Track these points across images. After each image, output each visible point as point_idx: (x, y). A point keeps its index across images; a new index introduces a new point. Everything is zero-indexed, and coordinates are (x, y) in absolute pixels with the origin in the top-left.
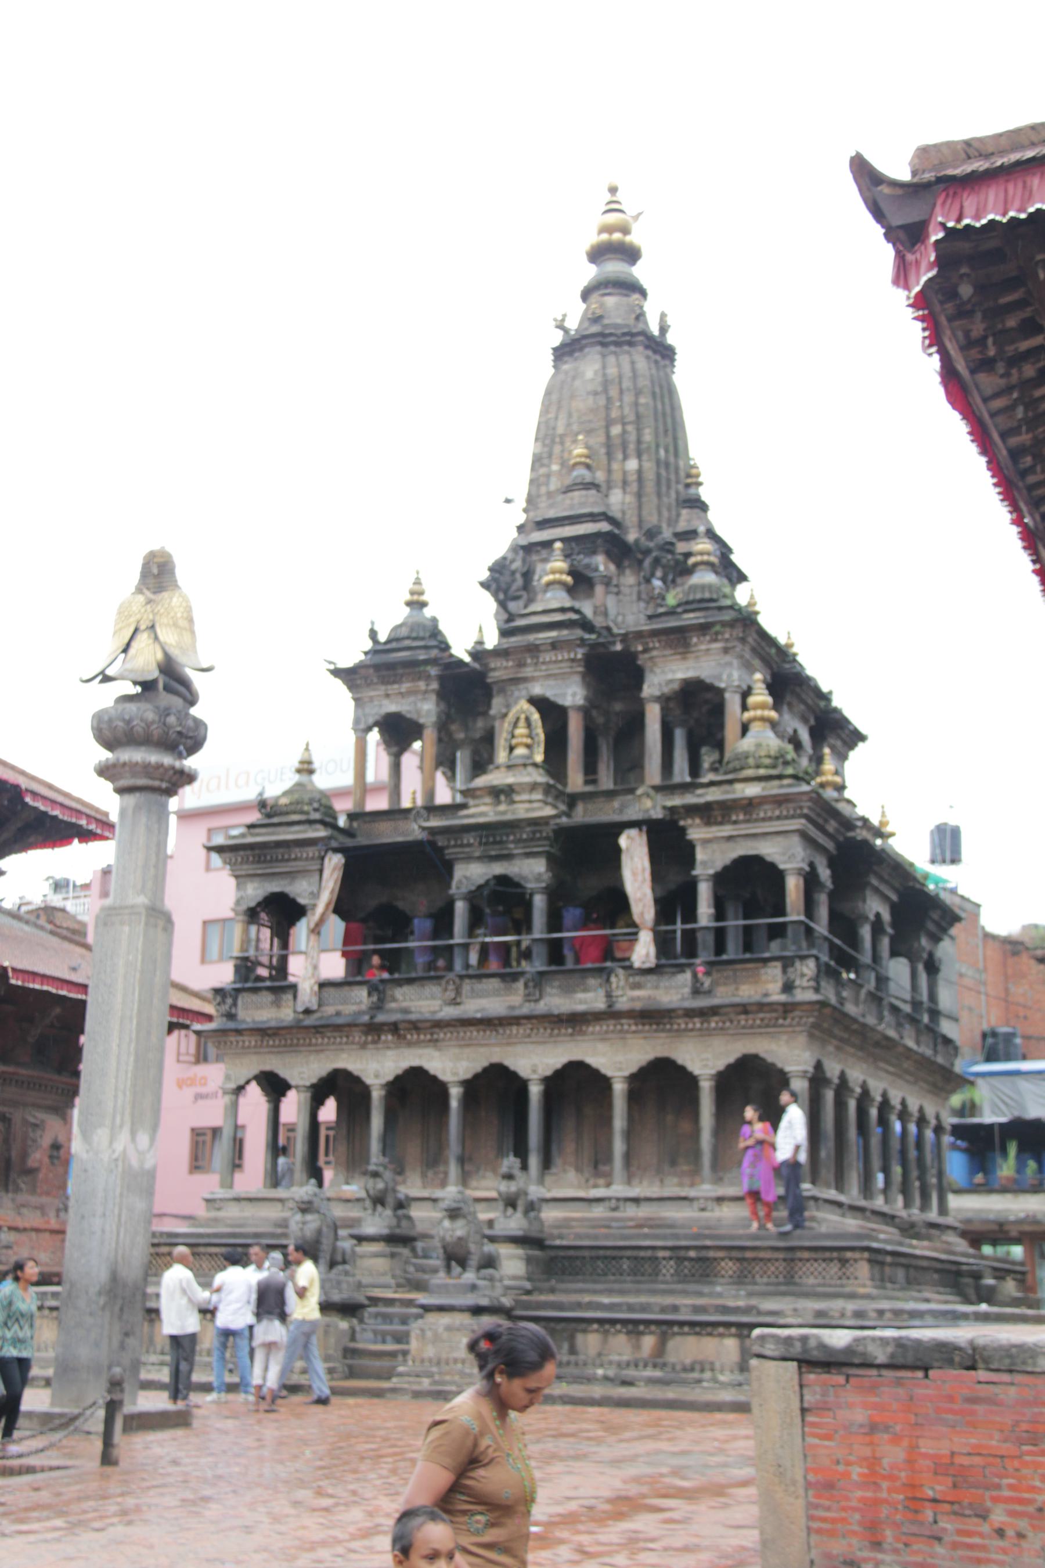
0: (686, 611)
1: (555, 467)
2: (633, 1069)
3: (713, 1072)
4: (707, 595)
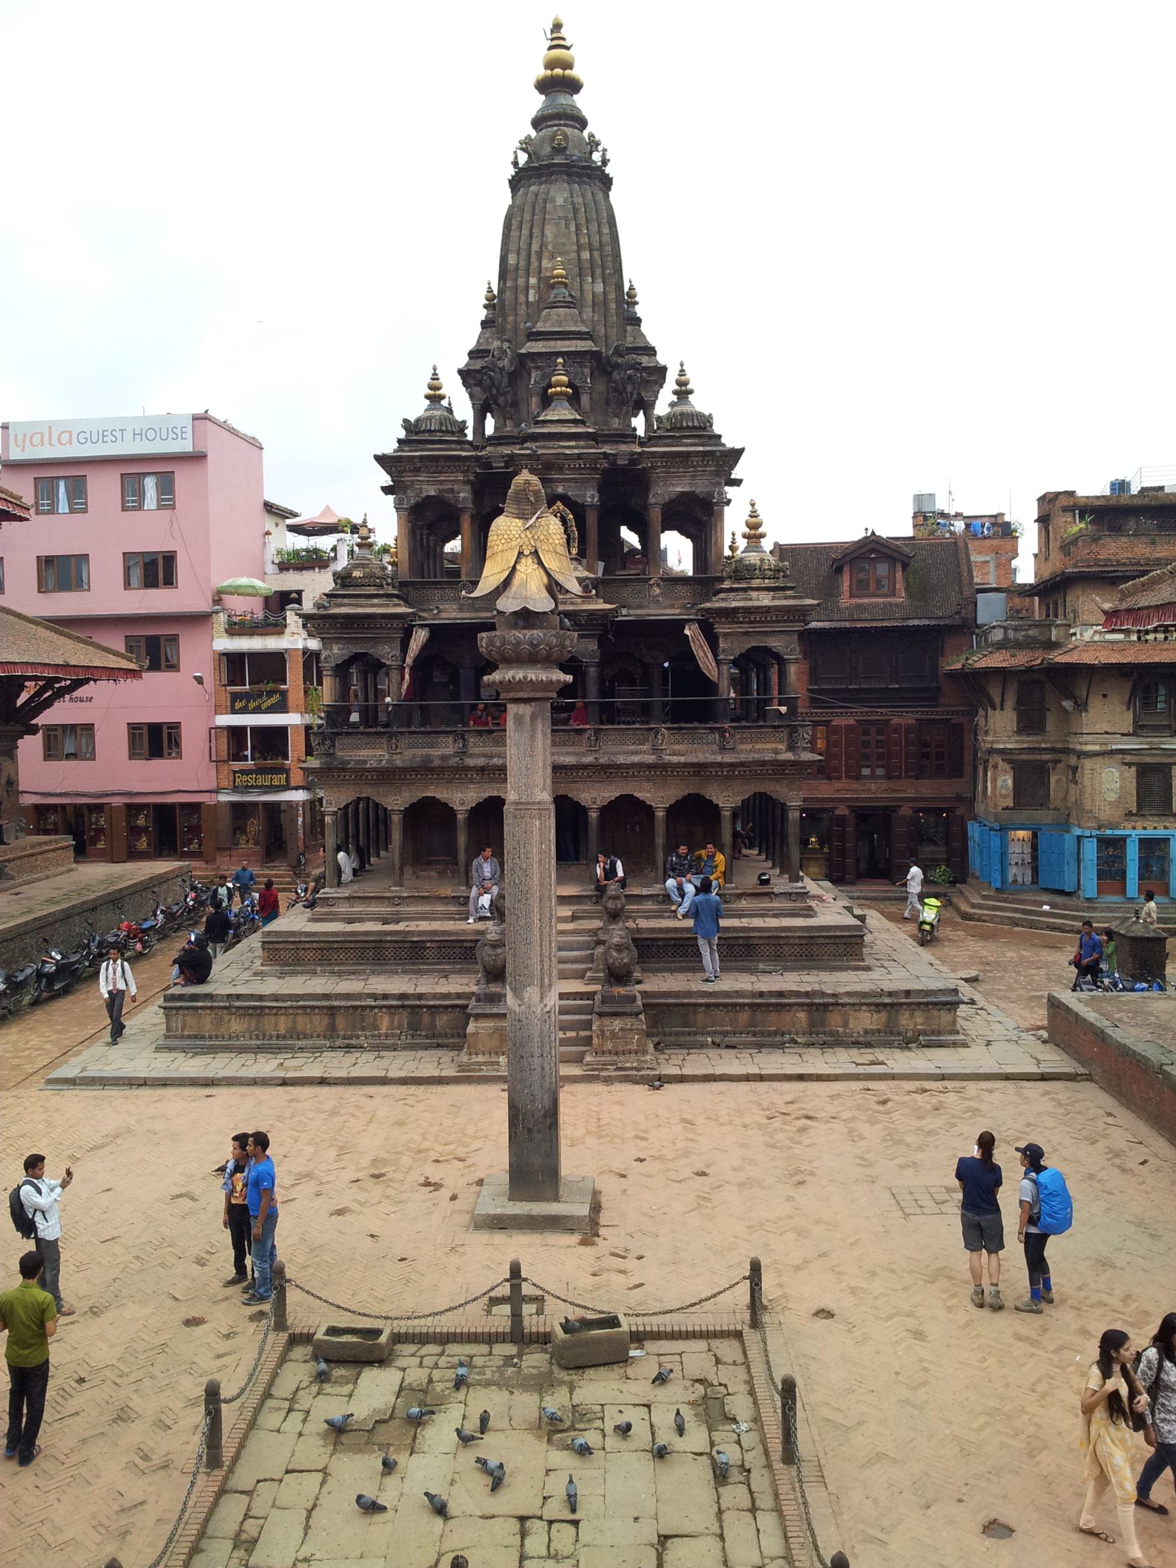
1: (533, 281)
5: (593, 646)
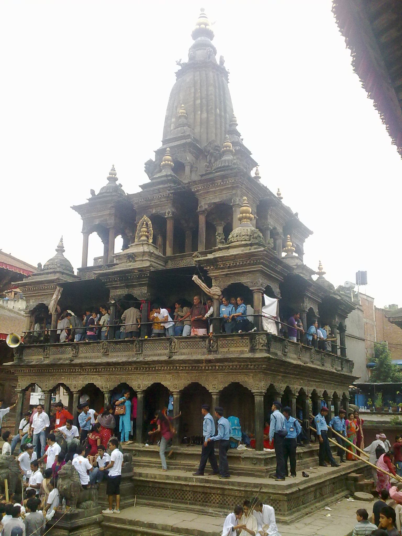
0: (216, 172)
1: (173, 120)
2: (182, 388)
3: (218, 391)
4: (227, 164)
5: (144, 290)
